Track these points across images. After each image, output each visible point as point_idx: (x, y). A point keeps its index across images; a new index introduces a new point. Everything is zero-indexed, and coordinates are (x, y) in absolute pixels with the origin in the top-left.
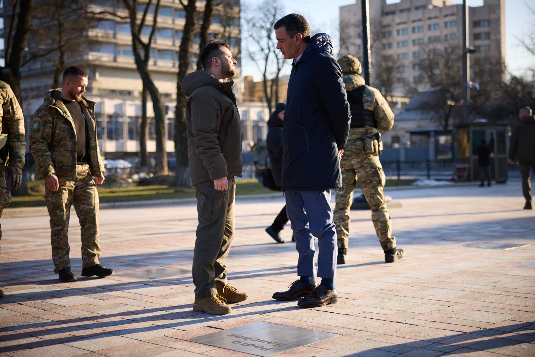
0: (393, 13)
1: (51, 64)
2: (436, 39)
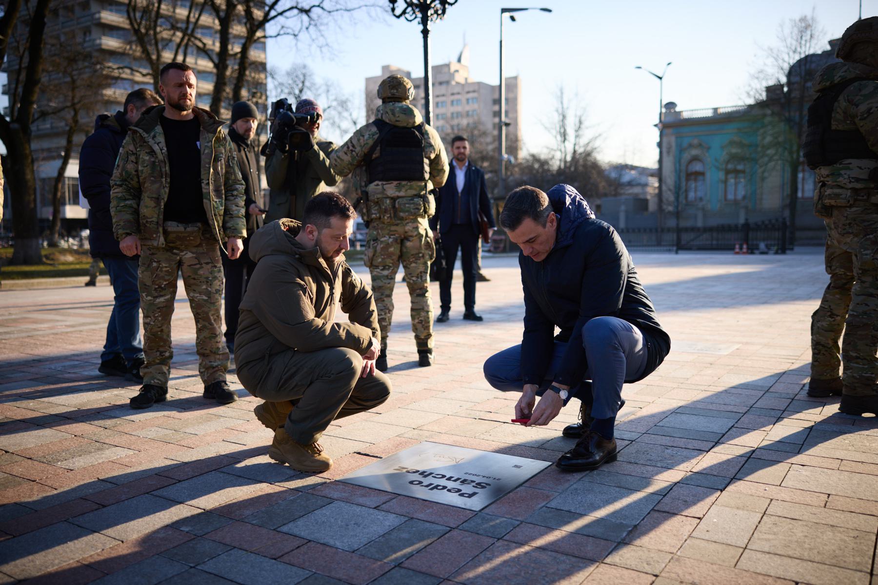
1: (63, 124)
2: (458, 115)
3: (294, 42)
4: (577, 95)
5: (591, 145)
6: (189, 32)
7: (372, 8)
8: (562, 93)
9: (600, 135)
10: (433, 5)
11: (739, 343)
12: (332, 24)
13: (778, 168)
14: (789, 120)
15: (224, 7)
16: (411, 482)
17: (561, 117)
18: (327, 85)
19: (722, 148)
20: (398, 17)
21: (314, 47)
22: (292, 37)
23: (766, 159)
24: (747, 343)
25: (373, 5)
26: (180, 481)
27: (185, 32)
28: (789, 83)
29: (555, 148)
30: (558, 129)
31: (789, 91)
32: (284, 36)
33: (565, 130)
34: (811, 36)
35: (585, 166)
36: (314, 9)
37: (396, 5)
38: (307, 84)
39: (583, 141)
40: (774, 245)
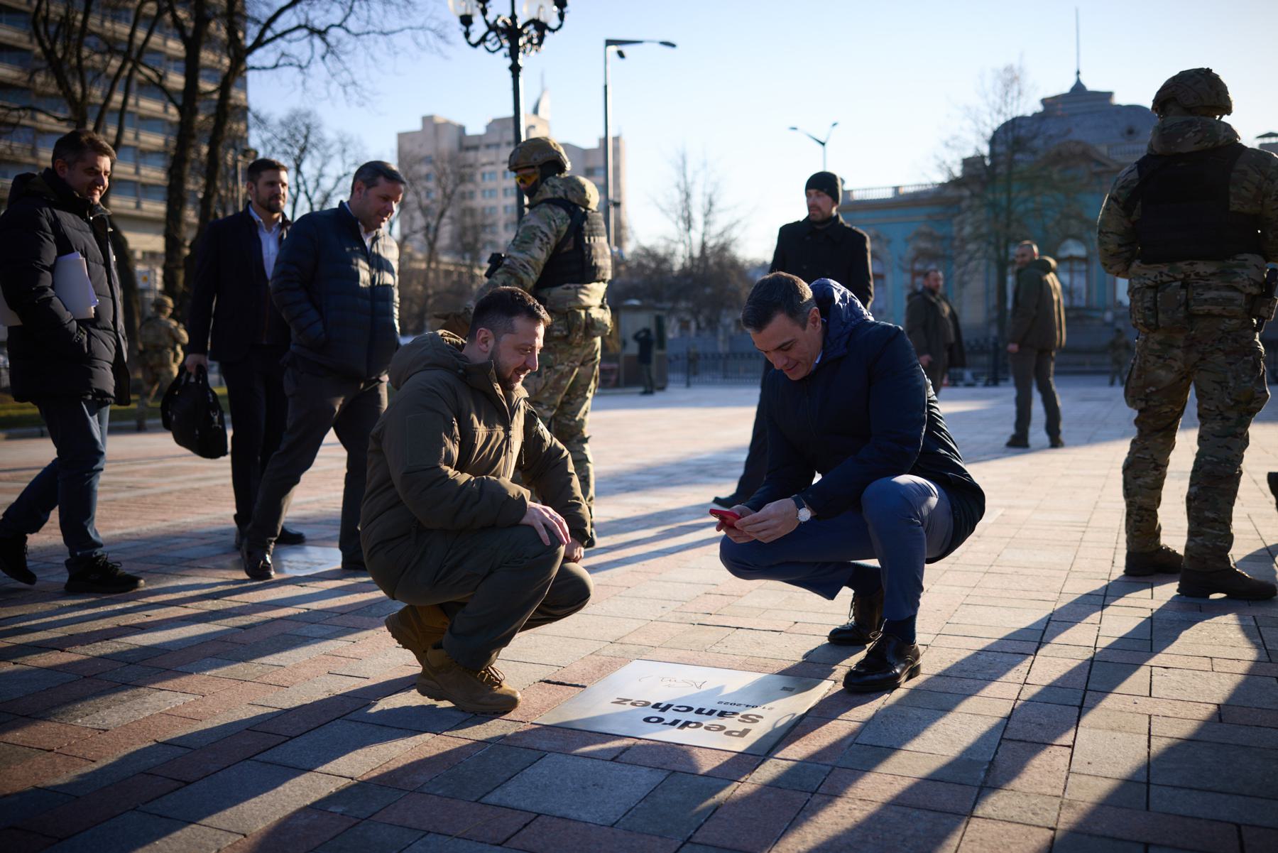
0: (476, 148)
3: (299, 78)
4: (705, 165)
5: (726, 235)
6: (134, 54)
7: (420, 32)
8: (684, 162)
9: (738, 222)
10: (525, 31)
11: (1000, 506)
12: (361, 52)
13: (982, 268)
14: (993, 205)
15: (192, 24)
16: (647, 720)
17: (684, 196)
18: (342, 142)
19: (907, 241)
20: (475, 45)
21: (334, 86)
22: (296, 70)
23: (965, 257)
24: (1010, 507)
25: (422, 28)
26: (291, 738)
27: (126, 57)
28: (993, 155)
29: (676, 239)
30: (680, 212)
31: (994, 165)
32: (285, 69)
33: (689, 214)
34: (1020, 93)
35: (719, 264)
36: (333, 31)
37: (471, 28)
38: (312, 139)
39: (715, 229)
40: (983, 374)
